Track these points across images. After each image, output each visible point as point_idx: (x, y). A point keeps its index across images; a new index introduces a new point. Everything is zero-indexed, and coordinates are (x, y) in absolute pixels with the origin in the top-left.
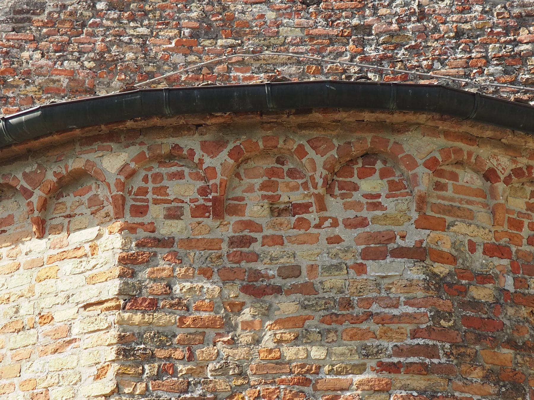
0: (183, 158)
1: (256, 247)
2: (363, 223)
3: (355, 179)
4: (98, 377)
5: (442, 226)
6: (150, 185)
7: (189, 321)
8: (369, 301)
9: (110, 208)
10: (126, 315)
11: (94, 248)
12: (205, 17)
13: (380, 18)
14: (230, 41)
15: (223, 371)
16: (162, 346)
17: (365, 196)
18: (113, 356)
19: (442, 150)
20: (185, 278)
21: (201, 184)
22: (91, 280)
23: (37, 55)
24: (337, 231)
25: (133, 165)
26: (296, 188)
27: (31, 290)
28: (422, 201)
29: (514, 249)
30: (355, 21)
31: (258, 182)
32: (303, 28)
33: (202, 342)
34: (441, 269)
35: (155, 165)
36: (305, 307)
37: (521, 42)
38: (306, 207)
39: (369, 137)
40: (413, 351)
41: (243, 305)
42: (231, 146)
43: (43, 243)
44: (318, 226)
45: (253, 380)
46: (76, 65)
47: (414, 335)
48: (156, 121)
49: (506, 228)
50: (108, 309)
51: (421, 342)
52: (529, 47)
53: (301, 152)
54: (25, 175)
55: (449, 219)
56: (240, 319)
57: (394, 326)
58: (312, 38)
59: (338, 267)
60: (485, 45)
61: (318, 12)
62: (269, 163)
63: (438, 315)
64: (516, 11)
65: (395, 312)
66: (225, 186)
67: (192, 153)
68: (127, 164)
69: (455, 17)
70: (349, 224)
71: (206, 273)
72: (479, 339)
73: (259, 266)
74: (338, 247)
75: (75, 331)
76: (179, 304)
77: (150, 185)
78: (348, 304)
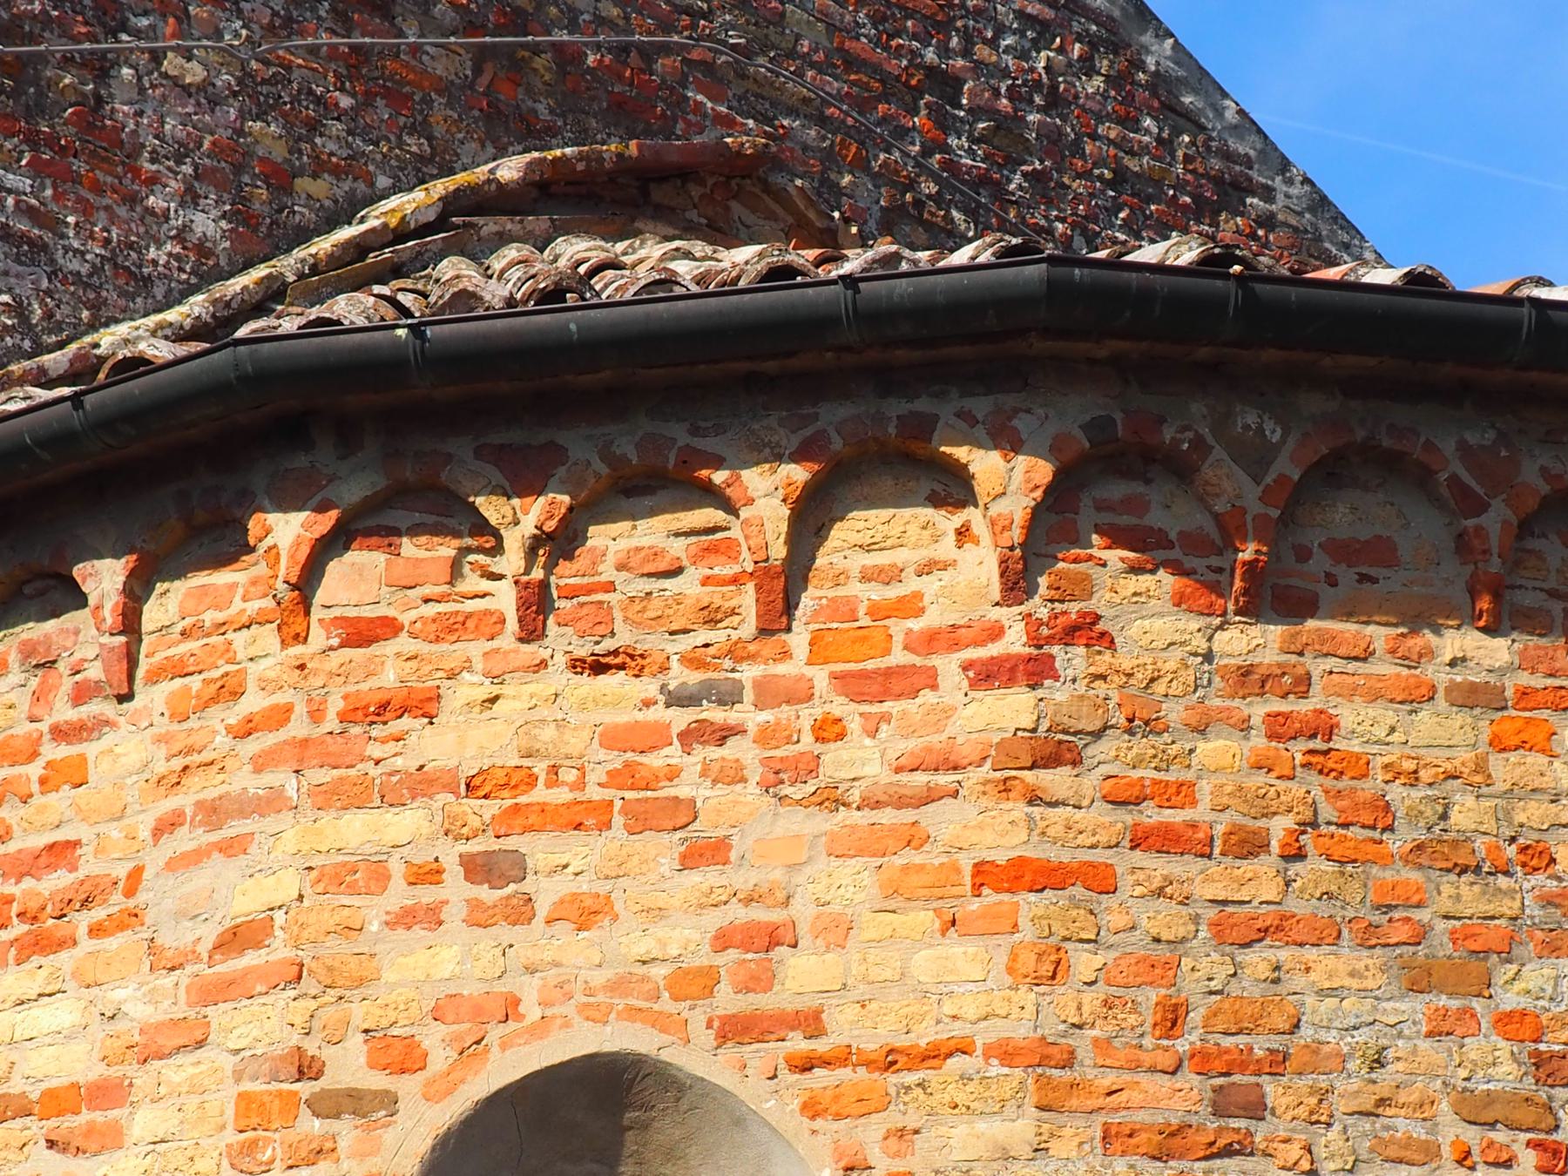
13: (979, 67)
32: (832, 28)
54: (1464, 449)
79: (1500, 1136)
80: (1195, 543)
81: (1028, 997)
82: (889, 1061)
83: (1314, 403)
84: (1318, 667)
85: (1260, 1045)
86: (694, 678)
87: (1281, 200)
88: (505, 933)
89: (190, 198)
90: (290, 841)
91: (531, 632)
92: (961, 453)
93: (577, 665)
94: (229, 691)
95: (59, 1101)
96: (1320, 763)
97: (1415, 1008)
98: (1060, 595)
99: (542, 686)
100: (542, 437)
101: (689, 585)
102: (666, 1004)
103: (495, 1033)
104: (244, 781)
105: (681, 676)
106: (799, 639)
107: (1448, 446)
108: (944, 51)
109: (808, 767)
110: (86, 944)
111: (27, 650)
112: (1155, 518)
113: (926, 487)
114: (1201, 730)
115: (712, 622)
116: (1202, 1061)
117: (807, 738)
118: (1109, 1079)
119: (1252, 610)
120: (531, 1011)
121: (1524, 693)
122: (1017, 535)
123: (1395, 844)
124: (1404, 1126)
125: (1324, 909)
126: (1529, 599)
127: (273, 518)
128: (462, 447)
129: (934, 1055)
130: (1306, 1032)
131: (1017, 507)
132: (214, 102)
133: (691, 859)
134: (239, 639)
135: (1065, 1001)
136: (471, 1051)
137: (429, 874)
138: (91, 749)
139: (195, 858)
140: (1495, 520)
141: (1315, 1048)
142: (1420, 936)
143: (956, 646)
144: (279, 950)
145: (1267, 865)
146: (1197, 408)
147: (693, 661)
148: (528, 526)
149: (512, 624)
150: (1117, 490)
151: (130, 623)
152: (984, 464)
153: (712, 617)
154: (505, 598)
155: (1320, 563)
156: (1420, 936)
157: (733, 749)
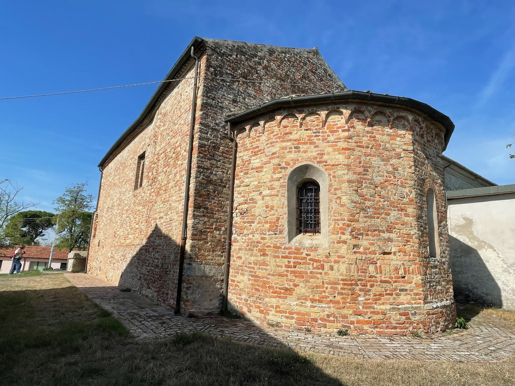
4: (409, 168)
22: (405, 144)
23: (274, 65)
43: (391, 131)
50: (410, 152)
54: (389, 112)
79: (390, 175)
80: (363, 119)
81: (347, 160)
82: (333, 165)
83: (376, 107)
84: (374, 131)
85: (368, 165)
86: (316, 131)
88: (298, 153)
89: (267, 96)
90: (278, 145)
91: (301, 127)
92: (342, 110)
93: (305, 130)
94: (273, 132)
95: (257, 168)
96: (374, 140)
97: (382, 163)
99: (302, 132)
100: (302, 109)
101: (315, 123)
102: (312, 160)
103: (297, 162)
104: (274, 140)
105: (314, 131)
106: (326, 128)
107: (388, 111)
108: (329, 89)
109: (326, 139)
110: (260, 155)
111: (255, 130)
112: (360, 117)
113: (338, 114)
114: (363, 137)
115: (317, 126)
116: (363, 166)
117: (326, 137)
118: (354, 168)
119: (368, 126)
120: (300, 160)
121: (393, 135)
122: (347, 118)
123: (381, 148)
125: (374, 153)
126: (394, 126)
127: (277, 117)
128: (295, 110)
129: (338, 165)
130: (372, 164)
131: (347, 115)
132: (270, 88)
133: (315, 147)
134: (274, 128)
135: (350, 161)
136: (294, 164)
137: (291, 148)
138: (260, 138)
139: (270, 147)
140: (392, 118)
141: (373, 166)
142: (383, 156)
143: (341, 128)
144: (277, 155)
145: (369, 149)
146: (364, 107)
147: (315, 129)
148: (301, 117)
149: (299, 126)
150: (356, 114)
151: (264, 127)
152: (344, 111)
153: (318, 126)
154: (298, 124)
155: (375, 122)
156: (383, 156)
157: (319, 137)
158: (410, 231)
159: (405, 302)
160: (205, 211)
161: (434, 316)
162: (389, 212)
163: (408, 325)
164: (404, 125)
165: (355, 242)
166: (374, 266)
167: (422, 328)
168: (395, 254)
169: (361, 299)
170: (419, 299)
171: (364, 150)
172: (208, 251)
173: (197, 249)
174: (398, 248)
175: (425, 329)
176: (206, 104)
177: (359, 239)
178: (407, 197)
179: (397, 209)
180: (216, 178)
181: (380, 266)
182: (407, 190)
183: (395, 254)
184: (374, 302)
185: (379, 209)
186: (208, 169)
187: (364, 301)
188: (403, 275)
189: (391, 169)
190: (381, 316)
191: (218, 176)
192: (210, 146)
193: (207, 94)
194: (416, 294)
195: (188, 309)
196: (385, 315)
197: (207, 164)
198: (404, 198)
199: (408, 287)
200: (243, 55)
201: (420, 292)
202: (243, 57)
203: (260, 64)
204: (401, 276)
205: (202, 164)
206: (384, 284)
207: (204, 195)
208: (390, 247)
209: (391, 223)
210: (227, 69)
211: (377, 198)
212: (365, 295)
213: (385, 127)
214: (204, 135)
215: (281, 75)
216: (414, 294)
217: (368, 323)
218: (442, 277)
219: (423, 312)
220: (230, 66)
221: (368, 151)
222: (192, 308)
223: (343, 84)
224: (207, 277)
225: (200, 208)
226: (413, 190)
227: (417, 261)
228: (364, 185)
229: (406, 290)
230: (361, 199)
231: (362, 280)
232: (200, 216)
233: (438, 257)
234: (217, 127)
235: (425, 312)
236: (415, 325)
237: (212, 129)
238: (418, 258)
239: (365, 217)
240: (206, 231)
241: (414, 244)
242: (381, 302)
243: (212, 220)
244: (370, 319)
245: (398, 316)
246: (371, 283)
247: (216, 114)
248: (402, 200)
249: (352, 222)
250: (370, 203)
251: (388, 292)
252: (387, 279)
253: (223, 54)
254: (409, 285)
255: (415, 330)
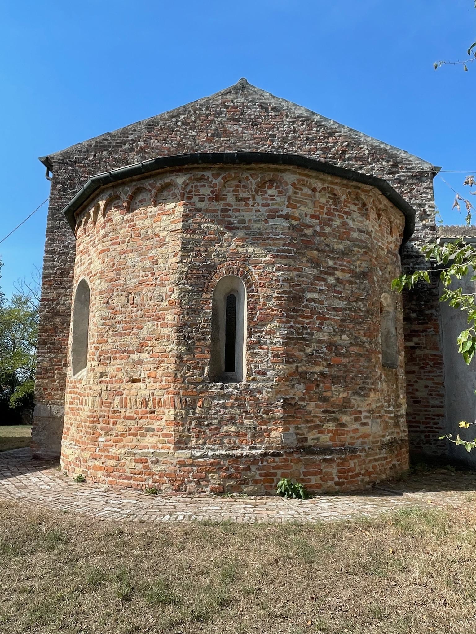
0: (205, 179)
1: (230, 213)
2: (268, 205)
3: (266, 189)
4: (174, 256)
5: (296, 207)
6: (194, 189)
7: (206, 238)
8: (269, 233)
9: (179, 197)
10: (184, 235)
11: (174, 211)
12: (216, 129)
13: (279, 132)
14: (225, 139)
15: (217, 256)
16: (197, 246)
17: (270, 196)
18: (180, 249)
19: (297, 180)
20: (205, 223)
21: (212, 189)
22: (172, 223)
23: (156, 142)
24: (259, 208)
25: (187, 181)
26: (245, 192)
27: (152, 225)
28: (289, 198)
29: (320, 216)
30: (270, 133)
31: (232, 189)
32: (252, 135)
33: (211, 246)
34: (294, 222)
35: (195, 182)
36: (246, 234)
37: (329, 143)
38: (248, 199)
39: (272, 174)
40: (283, 251)
41: (225, 233)
42: (222, 176)
43: (156, 209)
44: (252, 206)
45: (228, 259)
46: (170, 146)
47: (284, 245)
48: (196, 165)
49: (318, 209)
51: (286, 248)
52: (332, 144)
53: (247, 178)
54: (149, 184)
55: (298, 205)
56: (224, 238)
57: (277, 242)
58: (255, 138)
59: (259, 221)
60: (316, 143)
61: (257, 129)
62: (236, 182)
63: (293, 239)
64: (329, 131)
65: (278, 237)
66: (220, 190)
67: (208, 178)
68: (185, 181)
69: (306, 132)
70: (263, 206)
71: (213, 222)
72: (306, 247)
73: (231, 220)
74: (259, 213)
75: (167, 240)
76: (202, 232)
77: (194, 189)
78: (261, 234)
79: (147, 273)
85: (122, 267)
87: (343, 132)
98: (108, 217)
124: (137, 273)
158: (165, 347)
159: (149, 445)
160: (51, 346)
161: (195, 468)
162: (142, 324)
163: (146, 477)
164: (174, 194)
165: (101, 369)
166: (119, 397)
167: (167, 482)
168: (144, 381)
169: (101, 439)
170: (169, 443)
171: (118, 247)
172: (55, 390)
173: (42, 389)
174: (148, 372)
175: (173, 485)
176: (52, 228)
177: (107, 365)
178: (166, 299)
179: (152, 318)
180: (64, 308)
181: (126, 398)
182: (166, 290)
183: (144, 381)
184: (115, 444)
185: (130, 322)
186: (53, 300)
187: (105, 443)
188: (152, 409)
189: (149, 264)
190: (113, 462)
191: (67, 305)
192: (56, 274)
193: (53, 217)
194: (166, 435)
195: (33, 450)
196: (119, 460)
197: (53, 294)
198: (162, 301)
199: (156, 425)
200: (104, 150)
201: (171, 432)
202: (105, 152)
203: (132, 150)
204: (149, 410)
205: (47, 296)
206: (127, 421)
207: (50, 330)
208: (139, 373)
209: (144, 339)
210: (81, 177)
211: (130, 308)
212: (106, 434)
213: (149, 207)
214: (49, 263)
215: (169, 149)
216: (163, 434)
217: (100, 469)
218: (246, 412)
219: (172, 461)
220: (85, 172)
221: (124, 246)
222: (38, 450)
223: (308, 110)
224: (54, 418)
225: (45, 344)
226: (175, 288)
227: (171, 389)
228: (115, 294)
229: (153, 429)
230: (112, 313)
231: (104, 416)
232: (45, 353)
233: (244, 381)
234: (65, 250)
235: (175, 461)
236: (157, 477)
237: (60, 254)
238: (172, 384)
239: (113, 335)
240: (53, 369)
241: (169, 365)
242: (121, 444)
243: (60, 356)
244: (104, 465)
245: (134, 464)
246: (113, 420)
247: (65, 235)
248: (159, 306)
249: (100, 344)
250: (121, 315)
251: (132, 432)
252: (131, 415)
253: (75, 162)
254: (159, 423)
255: (156, 485)
